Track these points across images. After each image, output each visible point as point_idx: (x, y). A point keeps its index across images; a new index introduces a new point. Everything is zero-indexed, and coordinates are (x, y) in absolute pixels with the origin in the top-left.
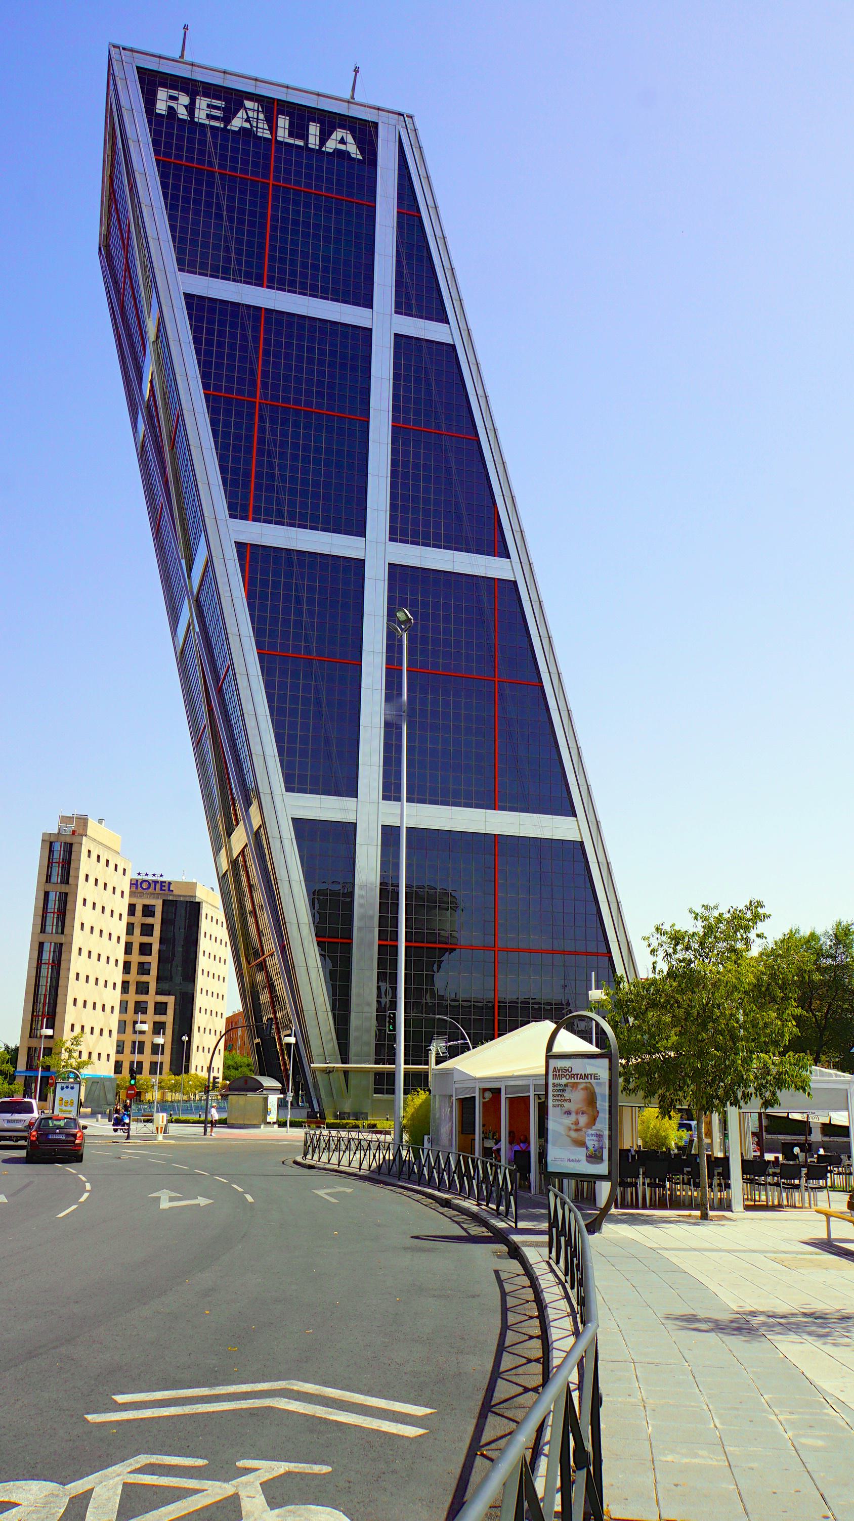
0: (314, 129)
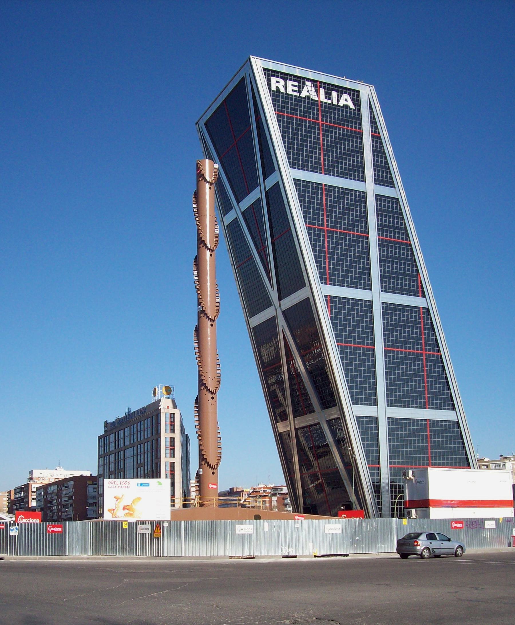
0: (334, 94)
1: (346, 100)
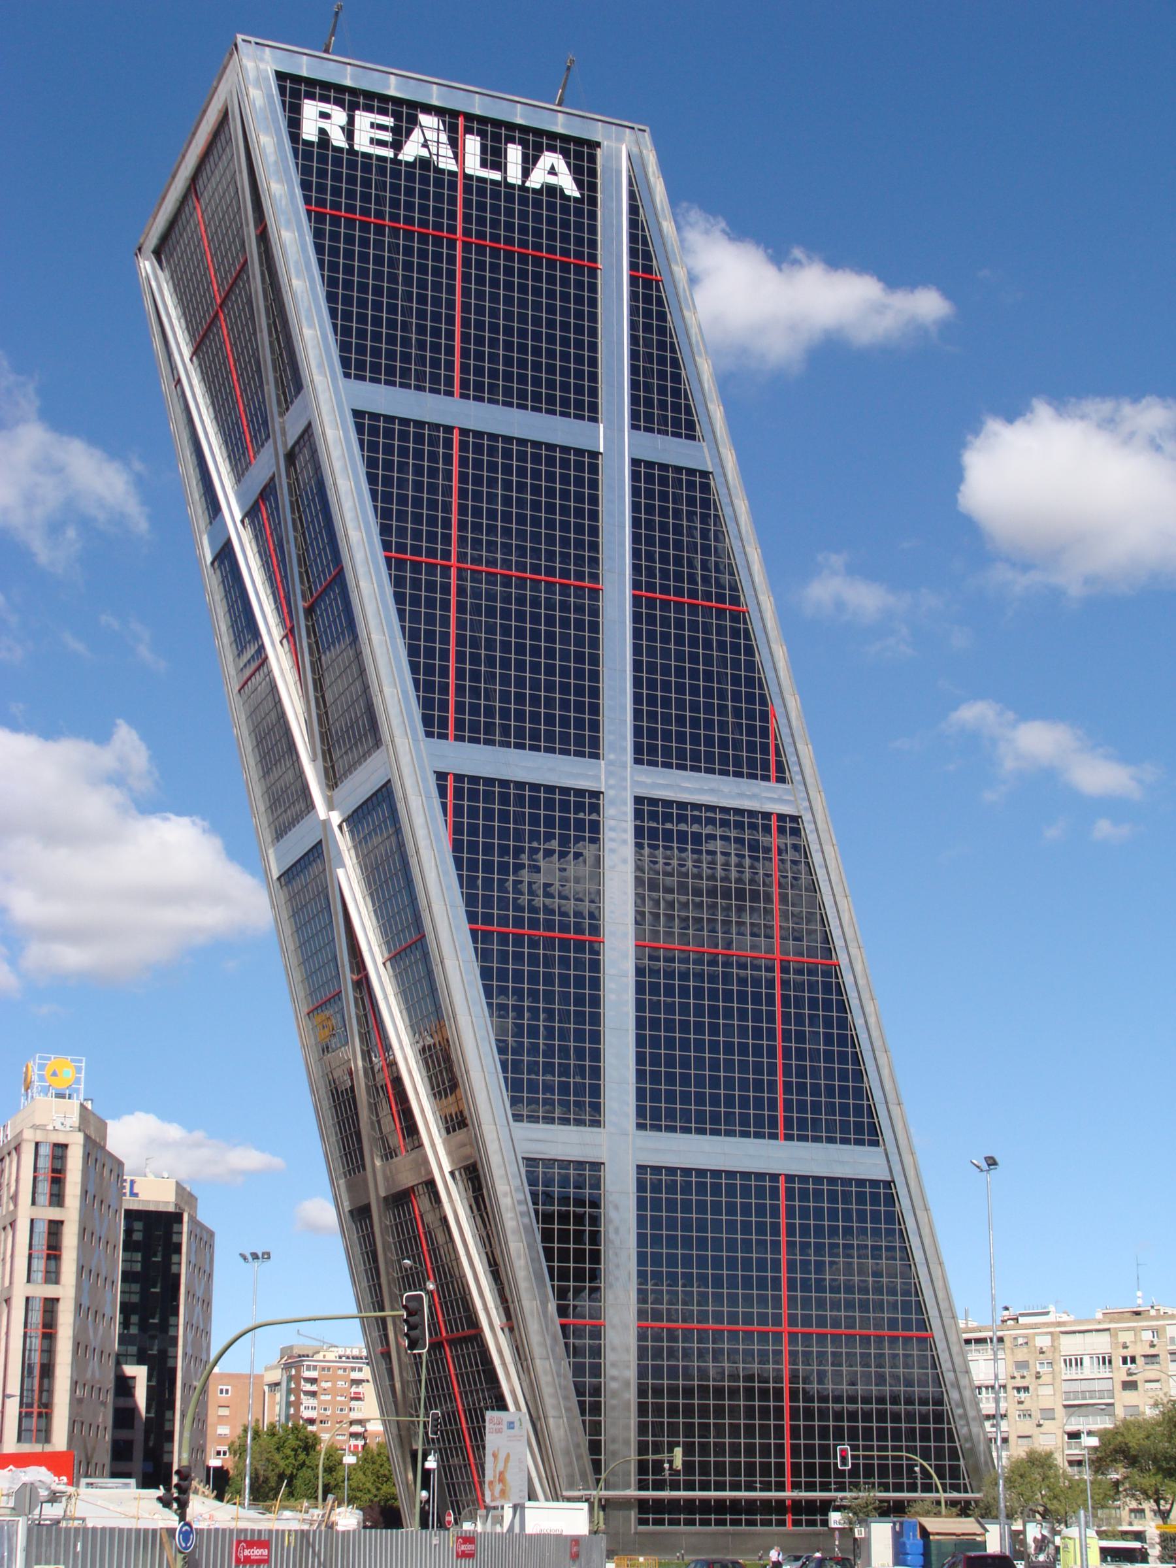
0: (514, 153)
1: (553, 172)
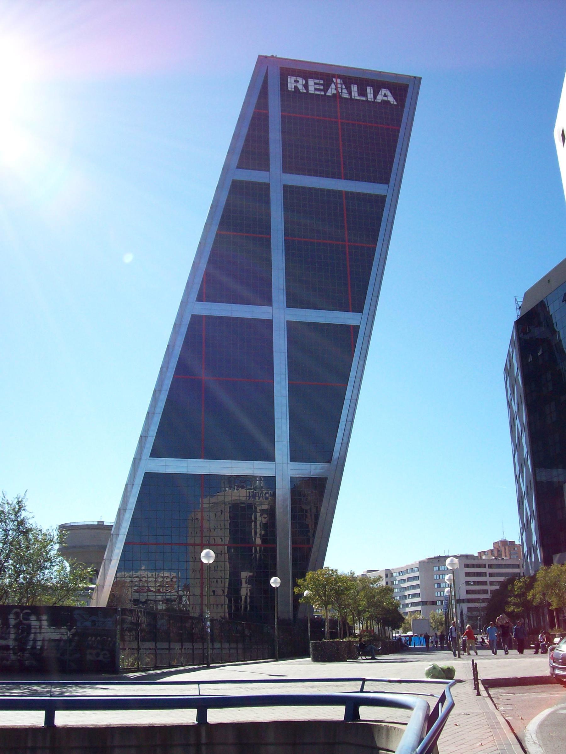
0: (370, 90)
1: (385, 96)
